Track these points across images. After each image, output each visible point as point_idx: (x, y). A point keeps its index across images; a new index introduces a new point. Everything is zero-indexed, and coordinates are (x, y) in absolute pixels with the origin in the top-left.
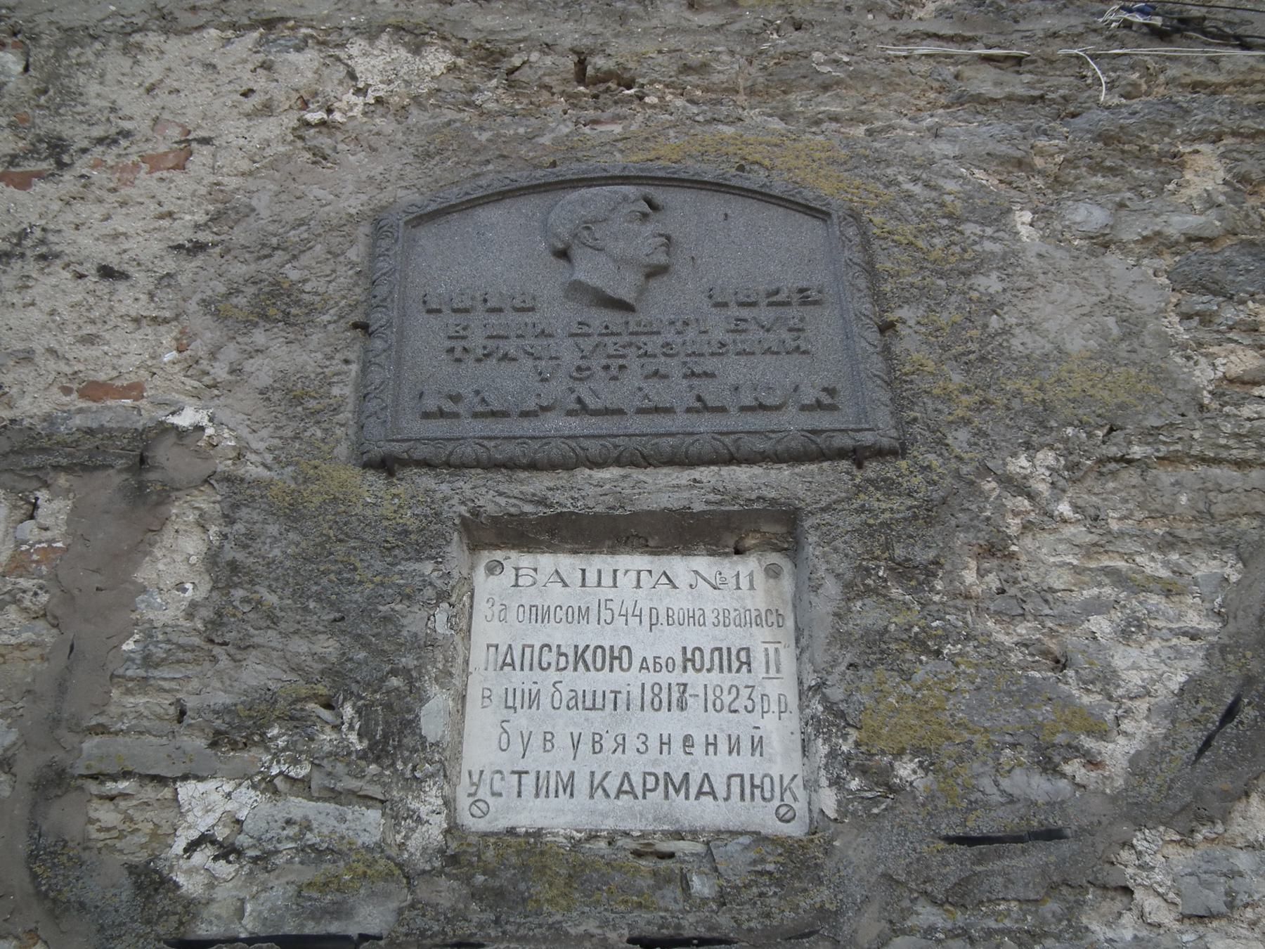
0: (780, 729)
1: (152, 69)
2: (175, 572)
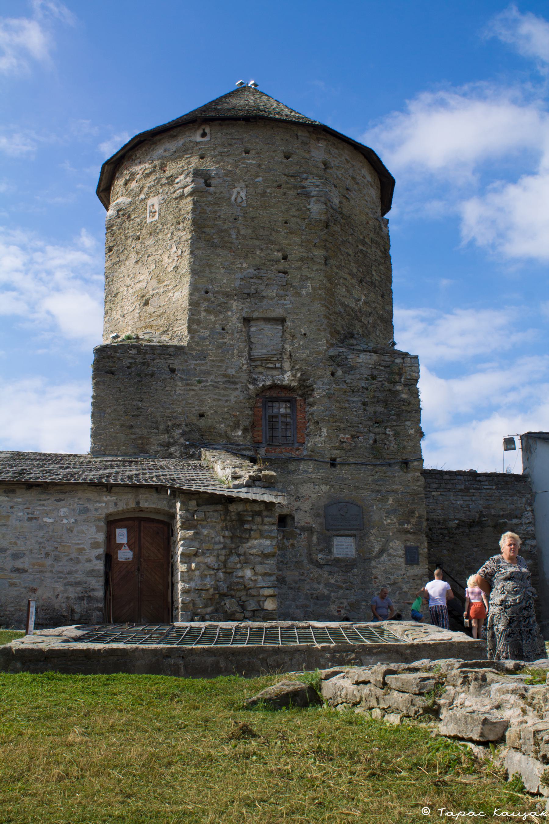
0: (353, 550)
1: (305, 488)
2: (315, 538)
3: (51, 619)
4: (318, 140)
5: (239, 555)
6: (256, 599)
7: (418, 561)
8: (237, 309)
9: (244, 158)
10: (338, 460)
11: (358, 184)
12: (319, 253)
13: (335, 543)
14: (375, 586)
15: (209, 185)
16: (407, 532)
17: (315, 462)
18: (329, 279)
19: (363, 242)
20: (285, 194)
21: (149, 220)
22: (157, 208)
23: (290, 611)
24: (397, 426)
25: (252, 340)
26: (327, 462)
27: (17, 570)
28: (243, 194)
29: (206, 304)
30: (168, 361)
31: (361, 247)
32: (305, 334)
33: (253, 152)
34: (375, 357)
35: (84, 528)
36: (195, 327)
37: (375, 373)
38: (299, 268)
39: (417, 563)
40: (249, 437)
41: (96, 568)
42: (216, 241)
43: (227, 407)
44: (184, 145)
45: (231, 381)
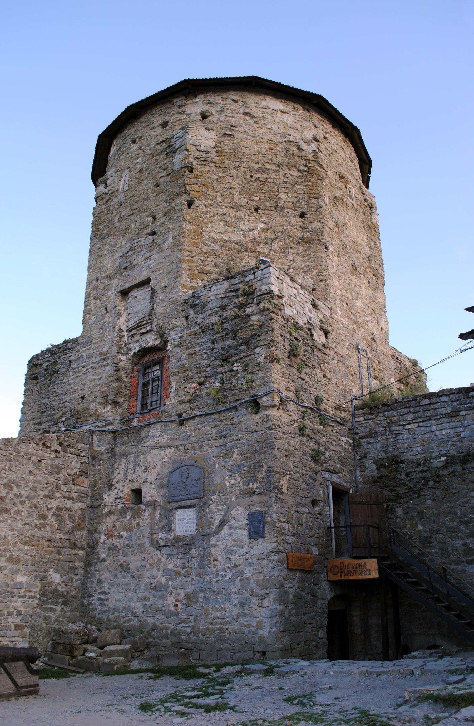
0: (195, 525)
2: (157, 515)
4: (196, 97)
7: (264, 533)
13: (177, 518)
14: (214, 570)
17: (162, 424)
20: (157, 160)
23: (132, 604)
24: (245, 357)
25: (129, 311)
26: (173, 421)
32: (166, 287)
33: (137, 140)
34: (226, 284)
37: (225, 301)
39: (263, 537)
43: (99, 385)
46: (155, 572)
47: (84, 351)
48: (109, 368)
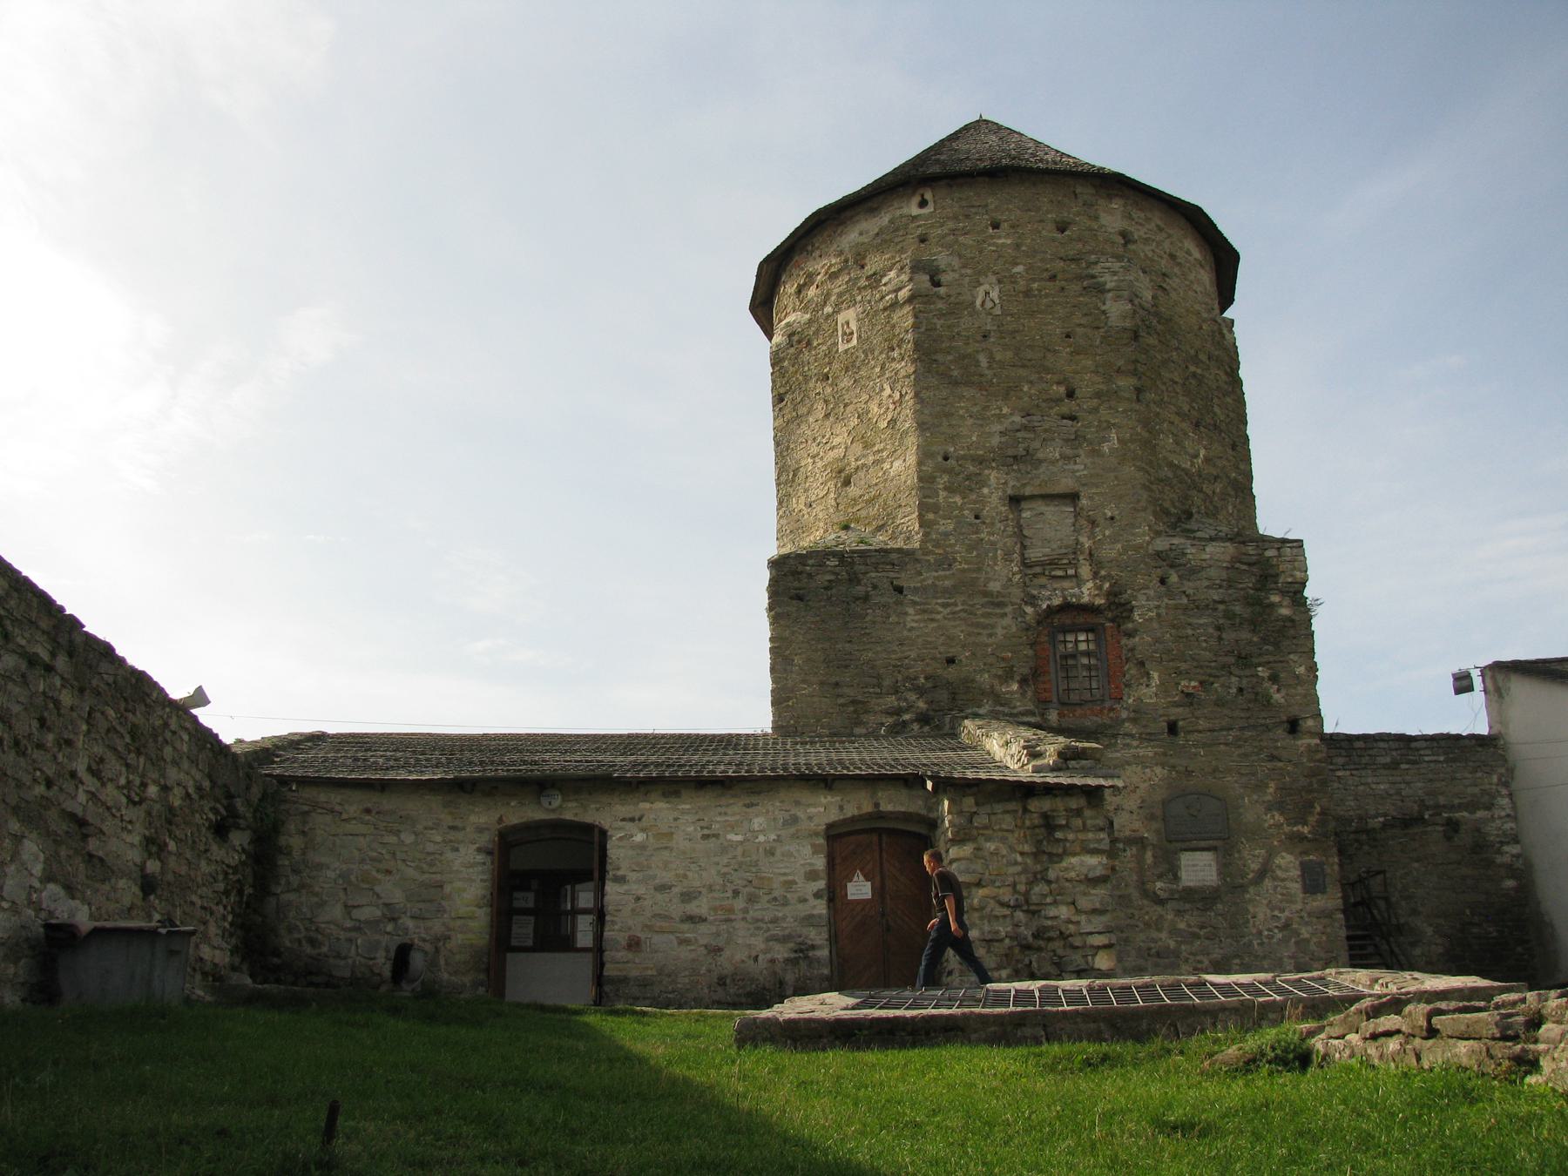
3: (749, 994)
4: (1110, 197)
5: (1049, 882)
6: (1080, 952)
8: (996, 484)
9: (992, 237)
10: (1181, 723)
11: (1179, 264)
12: (1125, 383)
15: (937, 284)
16: (1302, 838)
18: (1146, 424)
19: (1195, 360)
21: (841, 348)
22: (854, 327)
25: (1026, 532)
27: (691, 919)
28: (994, 295)
29: (946, 478)
30: (892, 575)
31: (1192, 369)
32: (1112, 518)
33: (1005, 225)
34: (1230, 548)
35: (792, 847)
36: (931, 516)
38: (1095, 410)
39: (1323, 892)
40: (1030, 693)
41: (815, 912)
42: (955, 373)
44: (891, 222)
45: (997, 602)
46: (1155, 934)
47: (937, 578)
48: (1007, 621)
